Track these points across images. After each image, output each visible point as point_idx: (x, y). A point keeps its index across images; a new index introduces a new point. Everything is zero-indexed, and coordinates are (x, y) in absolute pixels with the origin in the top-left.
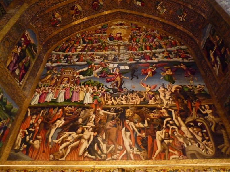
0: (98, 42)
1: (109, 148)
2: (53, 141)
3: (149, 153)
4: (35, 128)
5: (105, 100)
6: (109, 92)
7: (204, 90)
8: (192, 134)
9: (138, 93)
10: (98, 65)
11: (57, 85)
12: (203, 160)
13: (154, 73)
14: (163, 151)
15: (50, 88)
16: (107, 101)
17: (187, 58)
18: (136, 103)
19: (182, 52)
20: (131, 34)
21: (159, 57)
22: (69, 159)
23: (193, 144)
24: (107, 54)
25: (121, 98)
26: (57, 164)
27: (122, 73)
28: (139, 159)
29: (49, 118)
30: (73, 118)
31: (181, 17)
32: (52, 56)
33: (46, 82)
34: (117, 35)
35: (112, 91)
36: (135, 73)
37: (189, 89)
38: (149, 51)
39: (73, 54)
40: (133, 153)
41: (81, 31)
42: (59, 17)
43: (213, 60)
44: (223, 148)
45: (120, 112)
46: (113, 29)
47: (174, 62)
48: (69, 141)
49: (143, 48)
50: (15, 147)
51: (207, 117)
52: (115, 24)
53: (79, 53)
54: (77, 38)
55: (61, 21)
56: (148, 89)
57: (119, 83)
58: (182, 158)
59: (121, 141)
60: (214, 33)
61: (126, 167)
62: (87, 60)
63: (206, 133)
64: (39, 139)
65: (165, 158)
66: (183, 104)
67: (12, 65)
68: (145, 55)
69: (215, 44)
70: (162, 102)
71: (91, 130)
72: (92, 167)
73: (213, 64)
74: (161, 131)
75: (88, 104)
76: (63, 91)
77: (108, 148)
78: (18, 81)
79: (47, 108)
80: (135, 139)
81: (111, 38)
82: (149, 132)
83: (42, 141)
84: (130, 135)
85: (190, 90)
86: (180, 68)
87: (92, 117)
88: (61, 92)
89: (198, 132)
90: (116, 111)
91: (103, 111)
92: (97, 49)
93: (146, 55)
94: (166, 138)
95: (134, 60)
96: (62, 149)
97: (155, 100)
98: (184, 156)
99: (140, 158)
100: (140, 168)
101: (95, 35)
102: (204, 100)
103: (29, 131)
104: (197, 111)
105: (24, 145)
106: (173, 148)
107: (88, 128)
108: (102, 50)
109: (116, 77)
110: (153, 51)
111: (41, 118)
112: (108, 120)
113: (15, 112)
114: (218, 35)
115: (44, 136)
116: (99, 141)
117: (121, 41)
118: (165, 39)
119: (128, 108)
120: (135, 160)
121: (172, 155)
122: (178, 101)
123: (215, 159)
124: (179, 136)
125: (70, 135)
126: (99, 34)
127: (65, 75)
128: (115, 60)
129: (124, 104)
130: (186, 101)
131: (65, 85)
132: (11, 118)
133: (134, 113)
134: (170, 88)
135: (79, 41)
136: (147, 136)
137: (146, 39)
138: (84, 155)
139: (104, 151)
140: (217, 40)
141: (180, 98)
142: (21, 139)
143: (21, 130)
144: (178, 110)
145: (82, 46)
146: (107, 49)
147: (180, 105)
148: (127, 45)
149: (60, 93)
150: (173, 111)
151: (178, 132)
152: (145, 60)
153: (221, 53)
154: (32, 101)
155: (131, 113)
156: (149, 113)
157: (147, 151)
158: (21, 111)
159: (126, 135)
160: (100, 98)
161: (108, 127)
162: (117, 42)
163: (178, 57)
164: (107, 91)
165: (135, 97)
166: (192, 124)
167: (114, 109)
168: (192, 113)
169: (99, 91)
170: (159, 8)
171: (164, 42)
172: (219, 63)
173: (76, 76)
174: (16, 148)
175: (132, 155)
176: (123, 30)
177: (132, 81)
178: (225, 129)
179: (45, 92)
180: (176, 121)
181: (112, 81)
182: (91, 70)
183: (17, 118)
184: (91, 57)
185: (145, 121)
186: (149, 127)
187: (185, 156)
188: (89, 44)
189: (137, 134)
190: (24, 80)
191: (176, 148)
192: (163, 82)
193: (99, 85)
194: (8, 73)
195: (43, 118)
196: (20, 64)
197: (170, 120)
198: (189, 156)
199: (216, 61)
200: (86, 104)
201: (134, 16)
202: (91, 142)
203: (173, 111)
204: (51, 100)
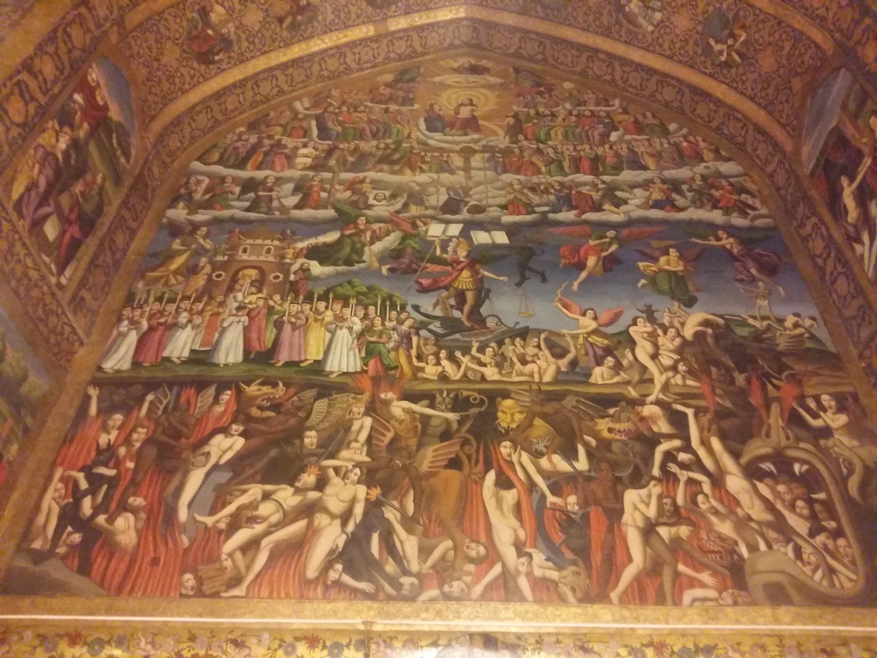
0: (380, 134)
3: (594, 577)
4: (118, 465)
5: (414, 360)
6: (430, 331)
7: (813, 337)
8: (770, 507)
9: (546, 340)
10: (382, 225)
11: (211, 298)
12: (817, 611)
13: (610, 263)
14: (654, 569)
15: (182, 305)
16: (421, 364)
17: (743, 209)
19: (723, 188)
20: (515, 108)
22: (265, 592)
23: (775, 547)
24: (419, 185)
26: (212, 614)
27: (481, 257)
29: (178, 425)
30: (281, 428)
31: (725, 47)
32: (193, 180)
33: (167, 284)
34: (457, 112)
35: (443, 326)
36: (534, 258)
37: (752, 330)
38: (589, 178)
40: (529, 575)
41: (311, 88)
42: (224, 23)
43: (853, 213)
45: (474, 411)
46: (444, 86)
47: (690, 223)
48: (265, 519)
49: (566, 164)
50: (32, 541)
51: (830, 442)
54: (296, 113)
56: (588, 323)
57: (470, 296)
58: (730, 601)
59: (482, 524)
61: (503, 630)
62: (338, 201)
63: (828, 504)
64: (134, 511)
65: (660, 600)
66: (732, 388)
67: (34, 198)
68: (574, 192)
70: (646, 376)
71: (356, 478)
72: (362, 627)
73: (851, 230)
74: (643, 492)
75: (344, 374)
76: (237, 319)
77: (424, 552)
78: (53, 267)
79: (171, 385)
81: (435, 122)
82: (595, 495)
83: (148, 519)
85: (757, 336)
86: (713, 246)
88: (230, 325)
90: (459, 404)
91: (406, 404)
93: (579, 193)
94: (661, 520)
95: (529, 208)
97: (618, 367)
98: (736, 592)
100: (557, 634)
101: (371, 109)
102: (815, 374)
104: (786, 416)
105: (70, 534)
106: (691, 557)
107: (344, 469)
108: (397, 168)
109: (455, 274)
110: (605, 178)
111: (143, 427)
115: (156, 500)
117: (476, 136)
119: (506, 395)
120: (538, 601)
122: (709, 375)
124: (716, 513)
125: (266, 496)
126: (385, 103)
127: (245, 257)
128: (451, 207)
129: (489, 379)
130: (743, 376)
131: (246, 295)
132: (18, 419)
133: (532, 415)
134: (677, 325)
135: (302, 127)
136: (588, 509)
138: (326, 578)
139: (408, 562)
141: (717, 364)
142: (56, 510)
143: (58, 473)
144: (712, 409)
146: (419, 164)
148: (501, 151)
149: (224, 330)
150: (690, 412)
151: (715, 498)
152: (575, 212)
155: (518, 417)
156: (592, 419)
159: (499, 502)
160: (392, 355)
161: (425, 467)
162: (457, 138)
163: (708, 207)
164: (423, 325)
165: (536, 355)
166: (768, 466)
167: (452, 395)
168: (769, 426)
169: (388, 324)
170: (632, 6)
171: (650, 145)
173: (291, 264)
174: (37, 545)
179: (162, 320)
180: (702, 453)
181: (439, 288)
183: (43, 423)
184: (353, 193)
185: (576, 451)
186: (593, 474)
187: (743, 593)
189: (543, 497)
191: (708, 559)
192: (648, 301)
193: (388, 303)
195: (152, 427)
196: (65, 201)
197: (679, 450)
198: (759, 594)
200: (335, 375)
201: (531, 39)
202: (357, 526)
203: (690, 412)
204: (186, 354)
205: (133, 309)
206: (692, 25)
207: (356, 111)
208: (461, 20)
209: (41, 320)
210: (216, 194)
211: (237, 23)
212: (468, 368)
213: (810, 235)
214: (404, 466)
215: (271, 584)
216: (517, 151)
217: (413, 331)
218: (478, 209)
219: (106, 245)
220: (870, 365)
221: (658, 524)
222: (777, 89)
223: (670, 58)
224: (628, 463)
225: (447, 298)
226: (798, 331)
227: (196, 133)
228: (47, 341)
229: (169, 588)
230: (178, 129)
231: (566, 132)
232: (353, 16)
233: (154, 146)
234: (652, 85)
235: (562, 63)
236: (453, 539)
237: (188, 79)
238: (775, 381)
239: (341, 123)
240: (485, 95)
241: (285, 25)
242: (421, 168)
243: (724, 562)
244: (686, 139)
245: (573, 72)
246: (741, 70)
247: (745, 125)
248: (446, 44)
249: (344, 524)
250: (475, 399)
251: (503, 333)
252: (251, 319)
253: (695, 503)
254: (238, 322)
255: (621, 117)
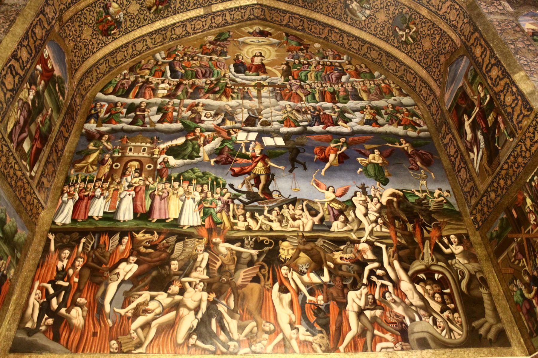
0: (207, 75)
1: (245, 328)
2: (114, 311)
6: (240, 200)
7: (448, 202)
8: (422, 298)
9: (306, 205)
10: (210, 133)
11: (113, 180)
12: (442, 351)
13: (342, 158)
14: (362, 333)
15: (97, 184)
17: (414, 126)
18: (304, 228)
19: (403, 113)
20: (286, 58)
21: (354, 120)
22: (156, 350)
24: (231, 107)
25: (268, 215)
27: (269, 154)
28: (311, 350)
32: (98, 105)
33: (87, 171)
34: (253, 61)
37: (417, 198)
38: (330, 105)
39: (148, 104)
40: (297, 339)
43: (469, 136)
44: (482, 326)
46: (245, 44)
47: (386, 134)
48: (153, 311)
49: (317, 95)
50: (26, 323)
51: (454, 262)
52: (249, 32)
53: (162, 102)
54: (157, 61)
55: (121, 23)
56: (330, 195)
57: (263, 178)
58: (399, 348)
59: (272, 313)
60: (474, 78)
62: (183, 118)
64: (81, 306)
65: (365, 349)
66: (406, 233)
67: (18, 131)
69: (476, 103)
70: (361, 227)
71: (201, 288)
73: (469, 144)
74: (358, 292)
75: (191, 227)
76: (128, 193)
77: (241, 328)
78: (28, 167)
80: (302, 308)
81: (240, 67)
82: (332, 294)
83: (89, 311)
84: (290, 299)
85: (420, 202)
87: (203, 259)
88: (124, 197)
89: (434, 294)
90: (258, 245)
92: (208, 92)
93: (324, 114)
94: (367, 307)
95: (296, 123)
96: (137, 329)
97: (346, 221)
98: (403, 343)
99: (313, 348)
101: (201, 58)
102: (447, 223)
103: (55, 287)
105: (46, 319)
106: (382, 326)
107: (194, 283)
108: (218, 96)
109: (254, 165)
110: (339, 105)
112: (239, 265)
113: (21, 240)
114: (480, 84)
116: (221, 313)
117: (264, 76)
118: (365, 77)
119: (284, 239)
121: (381, 341)
122: (394, 225)
123: (465, 349)
124: (395, 302)
125: (152, 298)
127: (131, 154)
128: (250, 121)
129: (274, 229)
131: (132, 178)
132: (13, 255)
133: (299, 251)
134: (378, 196)
135: (161, 70)
137: (324, 74)
140: (479, 93)
141: (398, 218)
142: (37, 306)
143: (37, 284)
144: (395, 245)
145: (170, 84)
146: (231, 94)
147: (399, 234)
148: (279, 86)
149: (122, 199)
150: (383, 247)
152: (322, 126)
153: (486, 123)
154: (57, 214)
155: (291, 252)
156: (332, 252)
157: (328, 334)
158: (33, 240)
159: (281, 300)
160: (219, 215)
161: (239, 282)
163: (396, 124)
164: (236, 197)
165: (301, 215)
166: (422, 276)
169: (216, 196)
170: (353, 5)
171: (364, 85)
172: (482, 145)
173: (158, 159)
174: (29, 325)
175: (294, 344)
176: (269, 48)
177: (292, 175)
178: (488, 288)
179: (86, 193)
182: (194, 145)
183: (26, 255)
184: (193, 113)
185: (322, 270)
186: (332, 283)
187: (406, 344)
188: (187, 79)
189: (305, 297)
190: (39, 166)
192: (363, 181)
194: (9, 150)
195: (86, 258)
196: (33, 128)
197: (377, 268)
199: (475, 140)
200: (186, 227)
201: (295, 18)
202: (203, 315)
203: (383, 247)
204: (101, 214)
205: (69, 186)
206: (386, 19)
207: (192, 59)
208: (255, 5)
209: (23, 198)
210: (112, 115)
211: (125, 12)
212: (262, 223)
213: (448, 144)
214: (228, 281)
215: (158, 345)
216: (288, 86)
217: (230, 200)
218: (266, 123)
219: (54, 149)
220: (475, 218)
221: (365, 310)
222: (432, 59)
223: (375, 35)
224: (350, 277)
225: (250, 180)
226: (441, 199)
227: (99, 76)
228: (26, 209)
229: (104, 349)
230: (90, 74)
231: (317, 75)
232: (192, 4)
233: (77, 87)
234: (365, 49)
235: (313, 32)
236: (256, 321)
237: (96, 46)
238: (427, 228)
239: (184, 68)
240: (269, 50)
241: (152, 11)
242: (232, 96)
243: (398, 328)
244: (384, 82)
245: (320, 38)
246: (413, 47)
247: (415, 77)
248: (246, 18)
249: (196, 314)
250: (267, 242)
251: (282, 201)
252: (137, 193)
253: (384, 297)
254: (130, 195)
255: (348, 67)
